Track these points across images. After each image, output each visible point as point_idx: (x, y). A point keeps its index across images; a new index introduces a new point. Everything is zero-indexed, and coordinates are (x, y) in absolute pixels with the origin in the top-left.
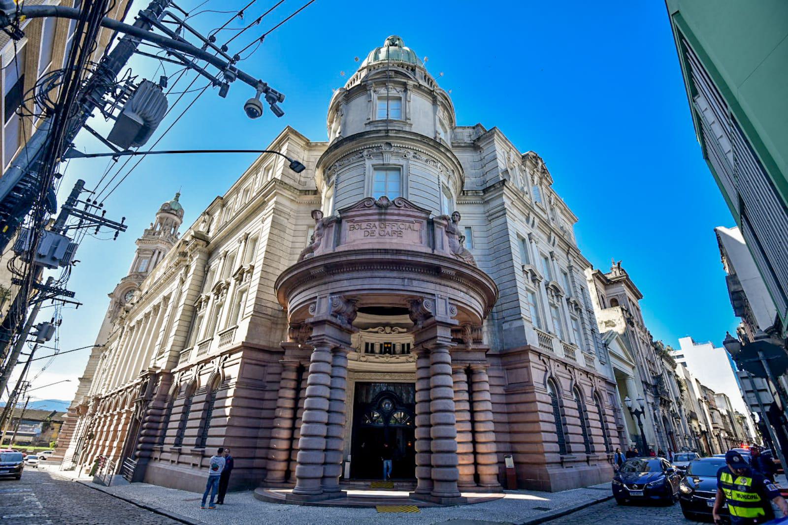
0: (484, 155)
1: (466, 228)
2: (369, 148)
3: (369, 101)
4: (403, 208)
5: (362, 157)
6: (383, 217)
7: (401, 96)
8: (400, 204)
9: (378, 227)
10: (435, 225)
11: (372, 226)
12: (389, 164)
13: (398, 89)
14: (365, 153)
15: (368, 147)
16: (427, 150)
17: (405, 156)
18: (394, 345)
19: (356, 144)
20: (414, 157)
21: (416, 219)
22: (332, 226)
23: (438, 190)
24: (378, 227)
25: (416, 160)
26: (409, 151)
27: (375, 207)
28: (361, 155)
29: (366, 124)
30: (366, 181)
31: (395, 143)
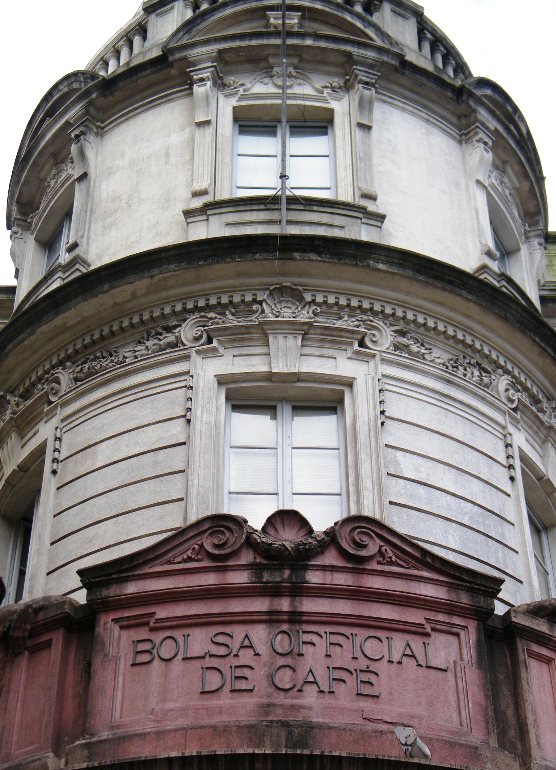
2: (208, 308)
3: (200, 125)
4: (374, 566)
5: (176, 344)
6: (285, 605)
7: (334, 105)
8: (361, 546)
9: (262, 648)
10: (521, 645)
11: (235, 645)
12: (298, 377)
13: (319, 81)
15: (201, 303)
16: (448, 322)
17: (362, 344)
19: (150, 291)
20: (397, 347)
21: (431, 615)
22: (48, 645)
23: (507, 486)
24: (262, 648)
26: (378, 323)
27: (246, 557)
28: (171, 338)
29: (188, 213)
31: (315, 290)
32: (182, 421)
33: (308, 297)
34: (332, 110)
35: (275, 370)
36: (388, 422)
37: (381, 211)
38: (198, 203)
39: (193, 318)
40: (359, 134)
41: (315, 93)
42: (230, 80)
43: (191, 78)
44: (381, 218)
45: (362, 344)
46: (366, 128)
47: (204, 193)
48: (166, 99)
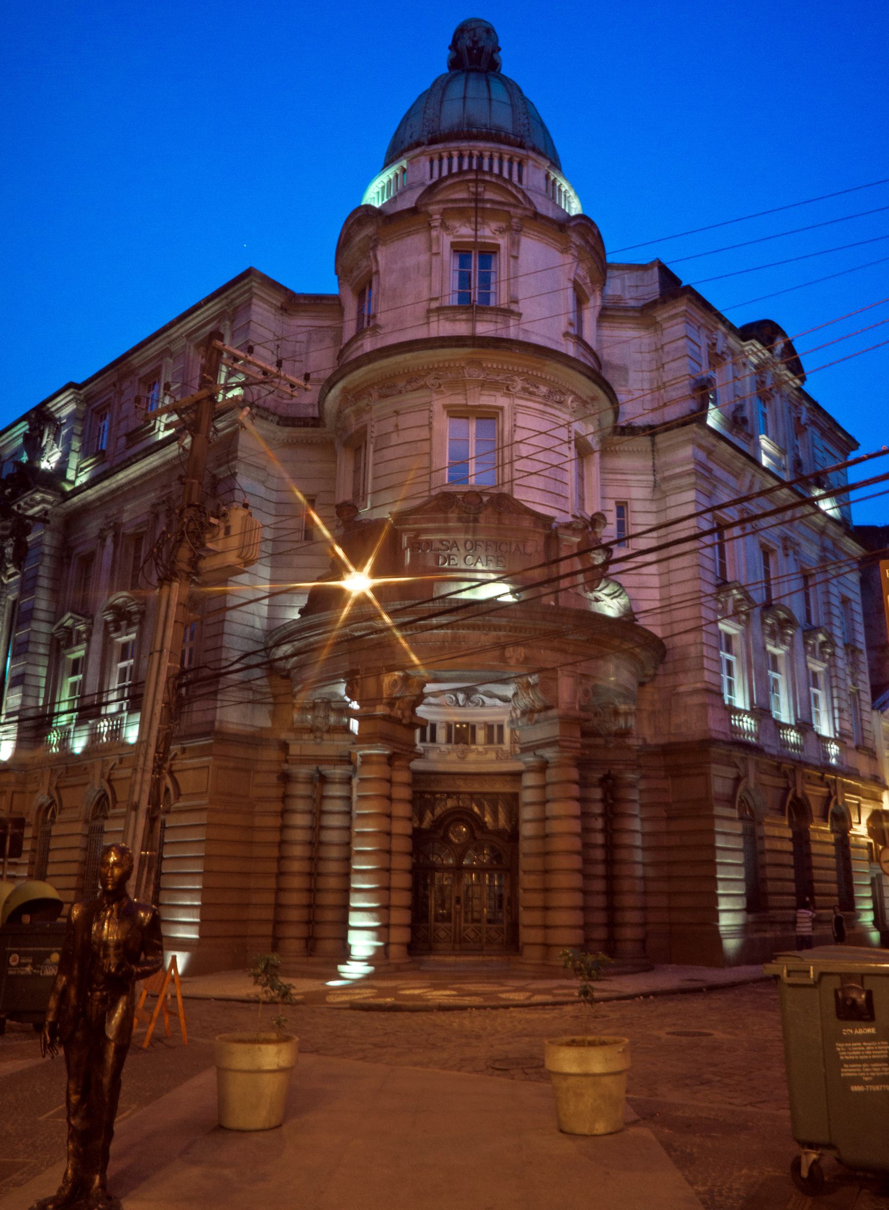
0: (665, 340)
1: (617, 503)
12: (479, 406)
13: (494, 225)
14: (430, 380)
17: (508, 389)
18: (473, 728)
20: (524, 389)
25: (527, 396)
26: (516, 378)
28: (423, 383)
29: (429, 311)
30: (435, 440)
32: (427, 428)
33: (484, 365)
34: (498, 246)
35: (469, 403)
36: (517, 429)
37: (521, 311)
38: (434, 305)
39: (433, 374)
40: (512, 260)
41: (490, 234)
42: (451, 223)
43: (430, 225)
44: (520, 315)
45: (508, 389)
46: (516, 258)
47: (437, 299)
48: (417, 232)
